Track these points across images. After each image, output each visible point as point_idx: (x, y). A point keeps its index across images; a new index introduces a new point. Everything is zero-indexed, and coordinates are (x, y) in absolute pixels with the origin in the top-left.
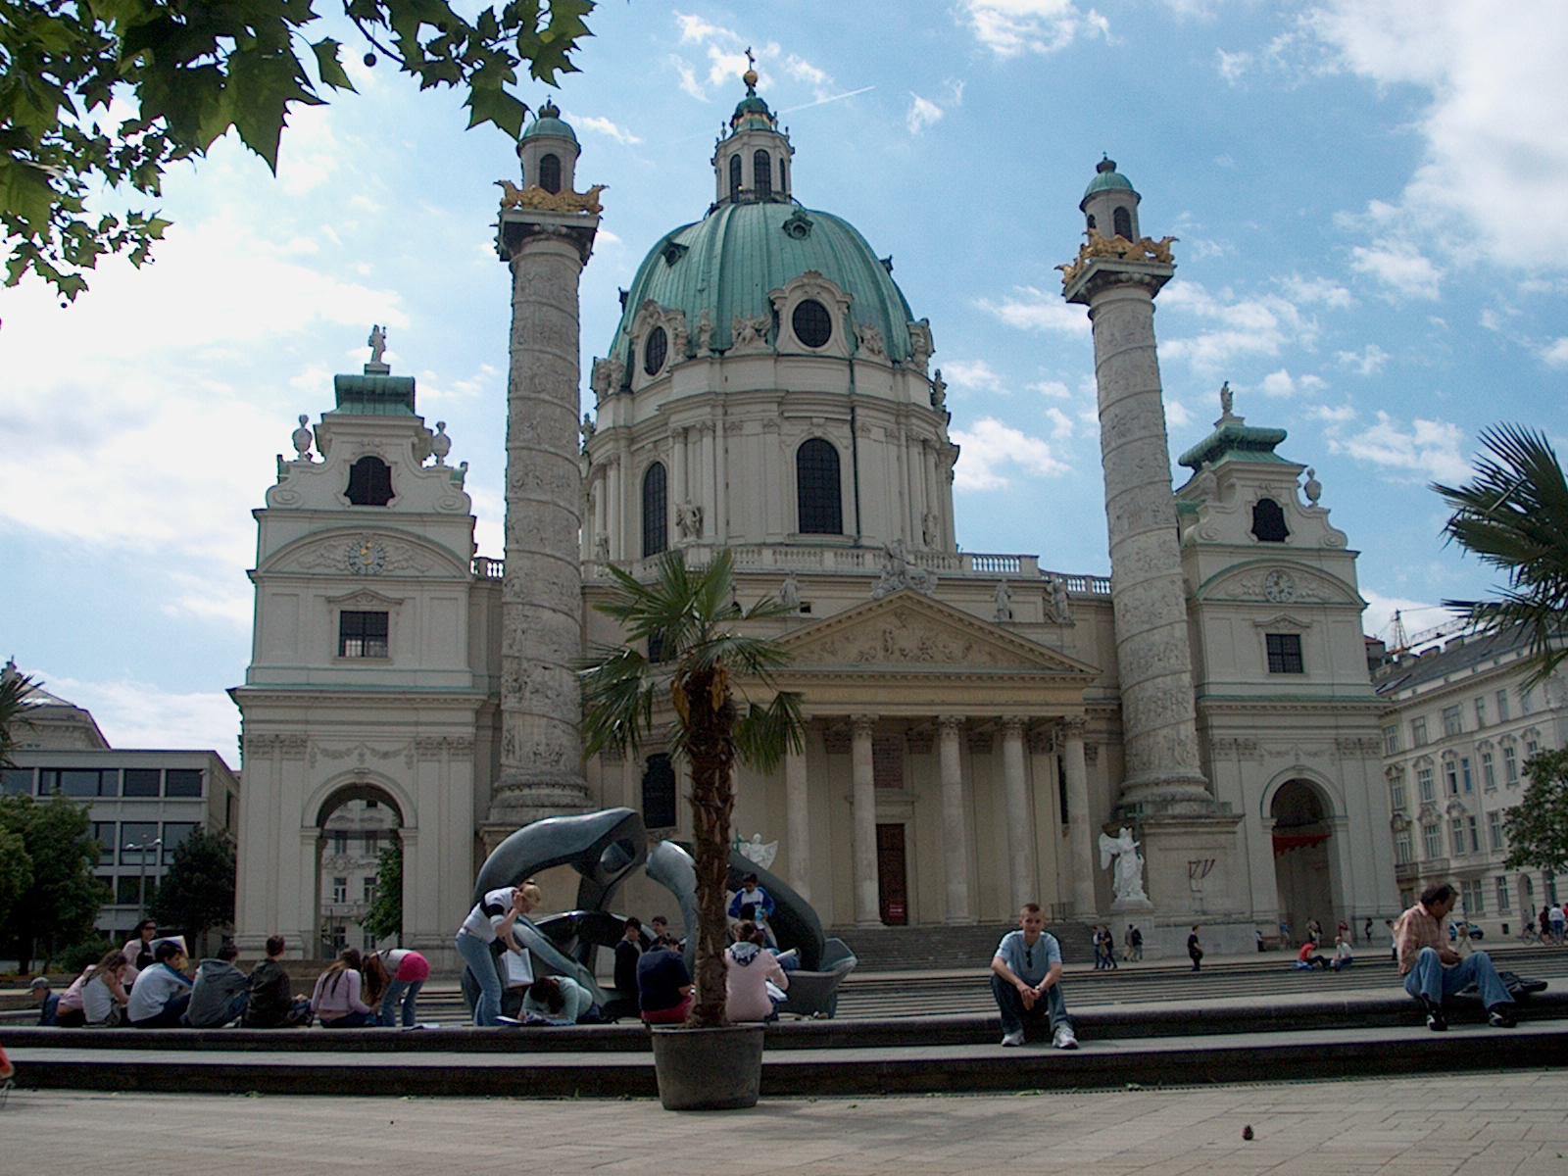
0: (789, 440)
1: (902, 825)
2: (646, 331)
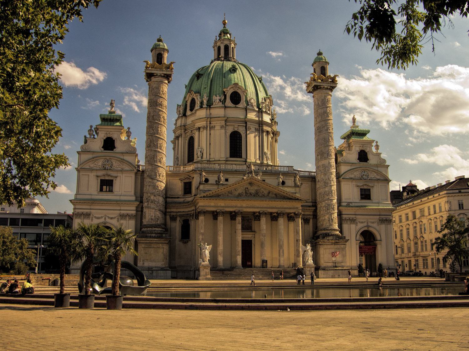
0: (228, 131)
1: (251, 240)
2: (190, 99)
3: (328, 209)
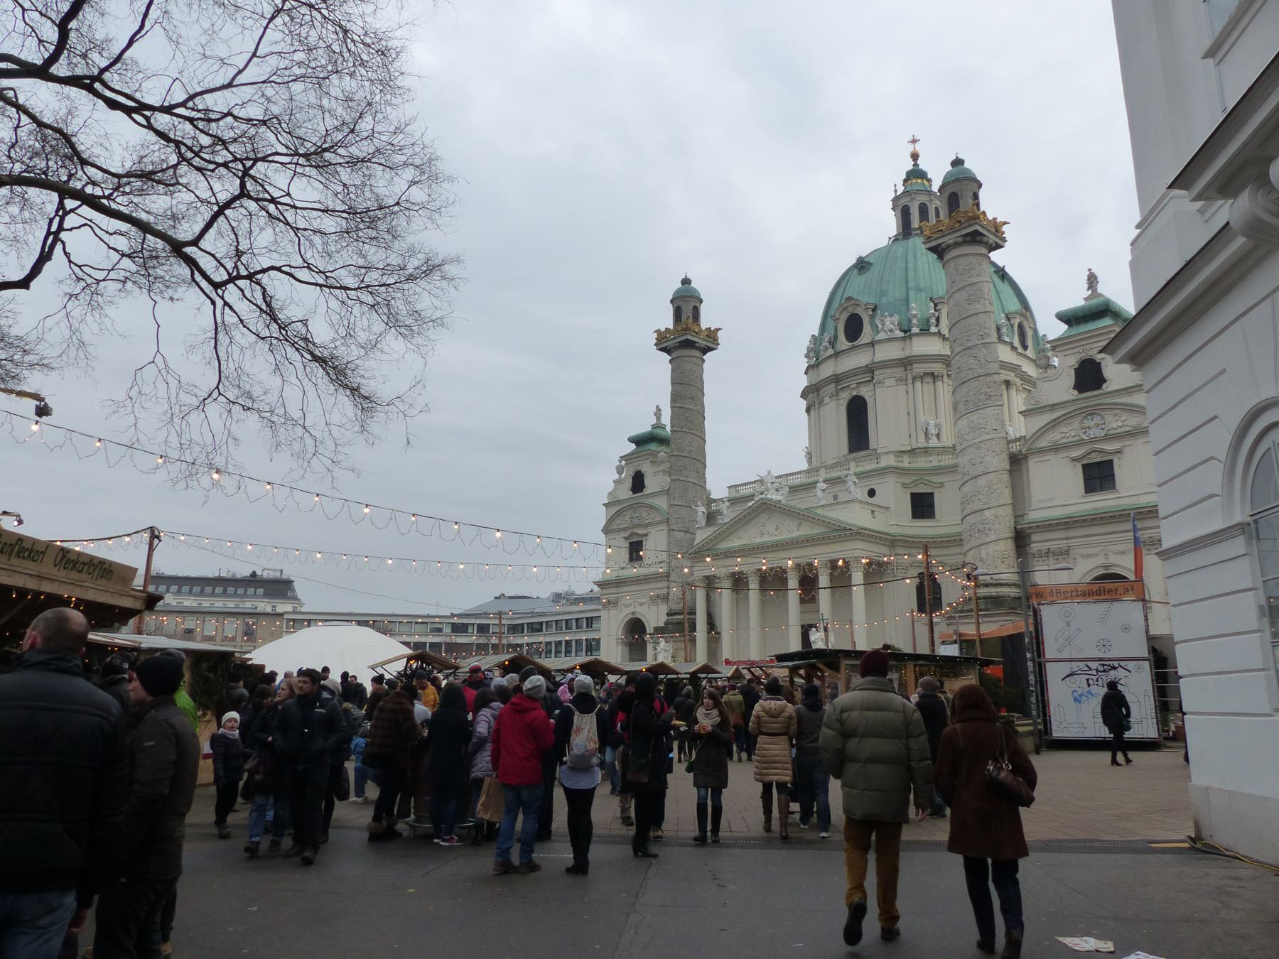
0: (841, 401)
3: (970, 536)
